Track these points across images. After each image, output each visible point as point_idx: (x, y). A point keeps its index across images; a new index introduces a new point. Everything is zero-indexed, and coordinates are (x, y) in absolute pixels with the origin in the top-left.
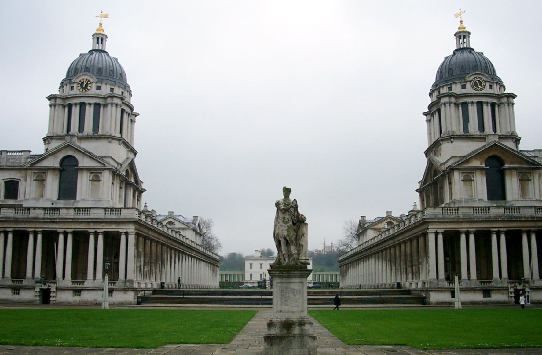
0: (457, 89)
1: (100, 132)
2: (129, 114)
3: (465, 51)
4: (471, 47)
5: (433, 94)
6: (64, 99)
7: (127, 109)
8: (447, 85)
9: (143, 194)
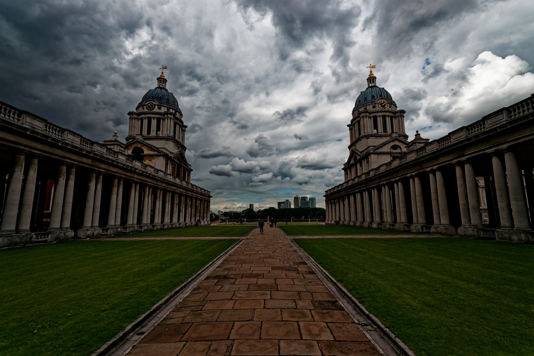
0: (370, 108)
6: (139, 114)
8: (364, 106)
9: (192, 172)
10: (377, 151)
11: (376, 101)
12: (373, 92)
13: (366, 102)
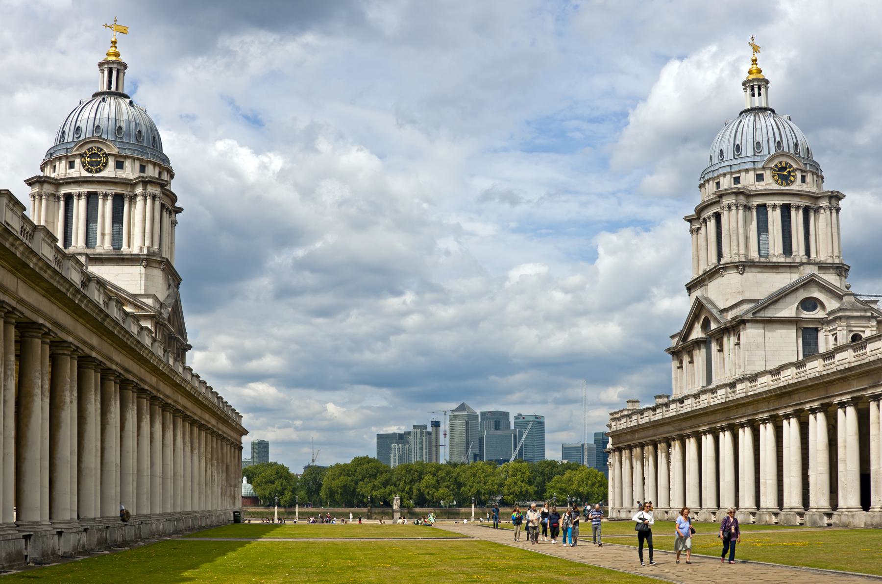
0: (748, 181)
1: (125, 249)
2: (170, 213)
3: (761, 115)
4: (770, 106)
5: (707, 185)
6: (57, 183)
7: (168, 204)
8: (731, 173)
12: (759, 132)
13: (738, 161)
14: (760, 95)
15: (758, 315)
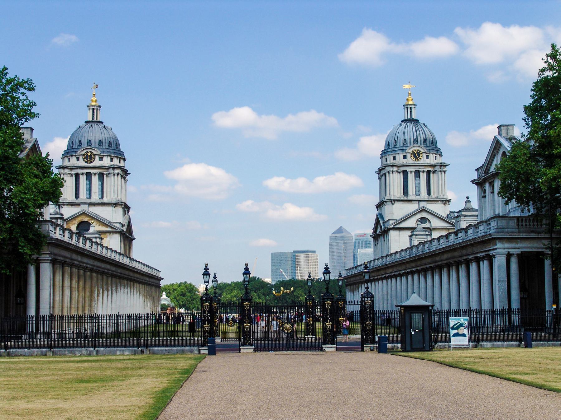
0: (400, 159)
6: (72, 168)
10: (398, 226)
11: (408, 148)
14: (411, 112)
15: (396, 226)
